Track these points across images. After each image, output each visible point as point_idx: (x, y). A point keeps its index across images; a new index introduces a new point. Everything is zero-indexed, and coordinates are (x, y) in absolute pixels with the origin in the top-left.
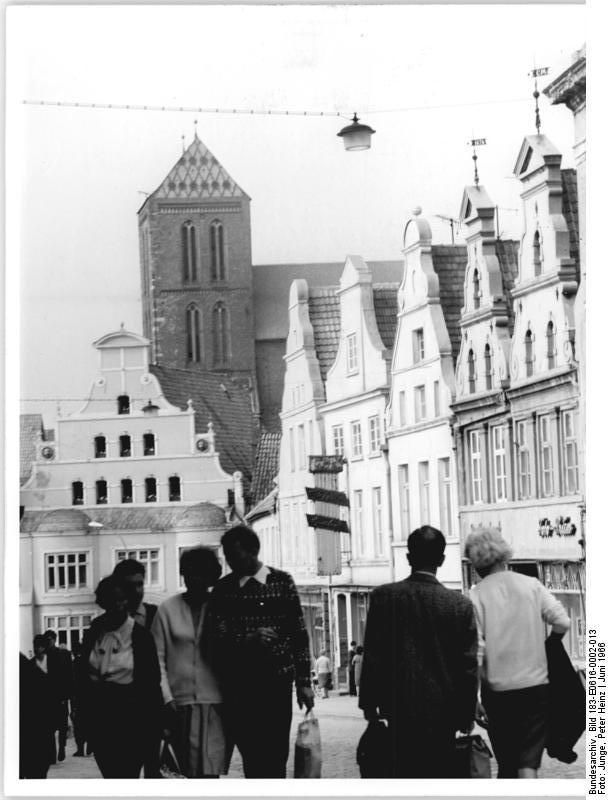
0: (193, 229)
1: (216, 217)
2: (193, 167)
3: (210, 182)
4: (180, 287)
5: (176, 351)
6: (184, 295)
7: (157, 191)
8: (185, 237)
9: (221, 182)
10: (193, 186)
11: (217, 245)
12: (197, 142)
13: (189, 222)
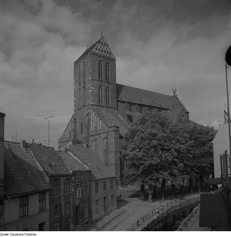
0: (101, 63)
1: (107, 62)
3: (106, 51)
4: (98, 79)
11: (107, 70)
13: (100, 61)
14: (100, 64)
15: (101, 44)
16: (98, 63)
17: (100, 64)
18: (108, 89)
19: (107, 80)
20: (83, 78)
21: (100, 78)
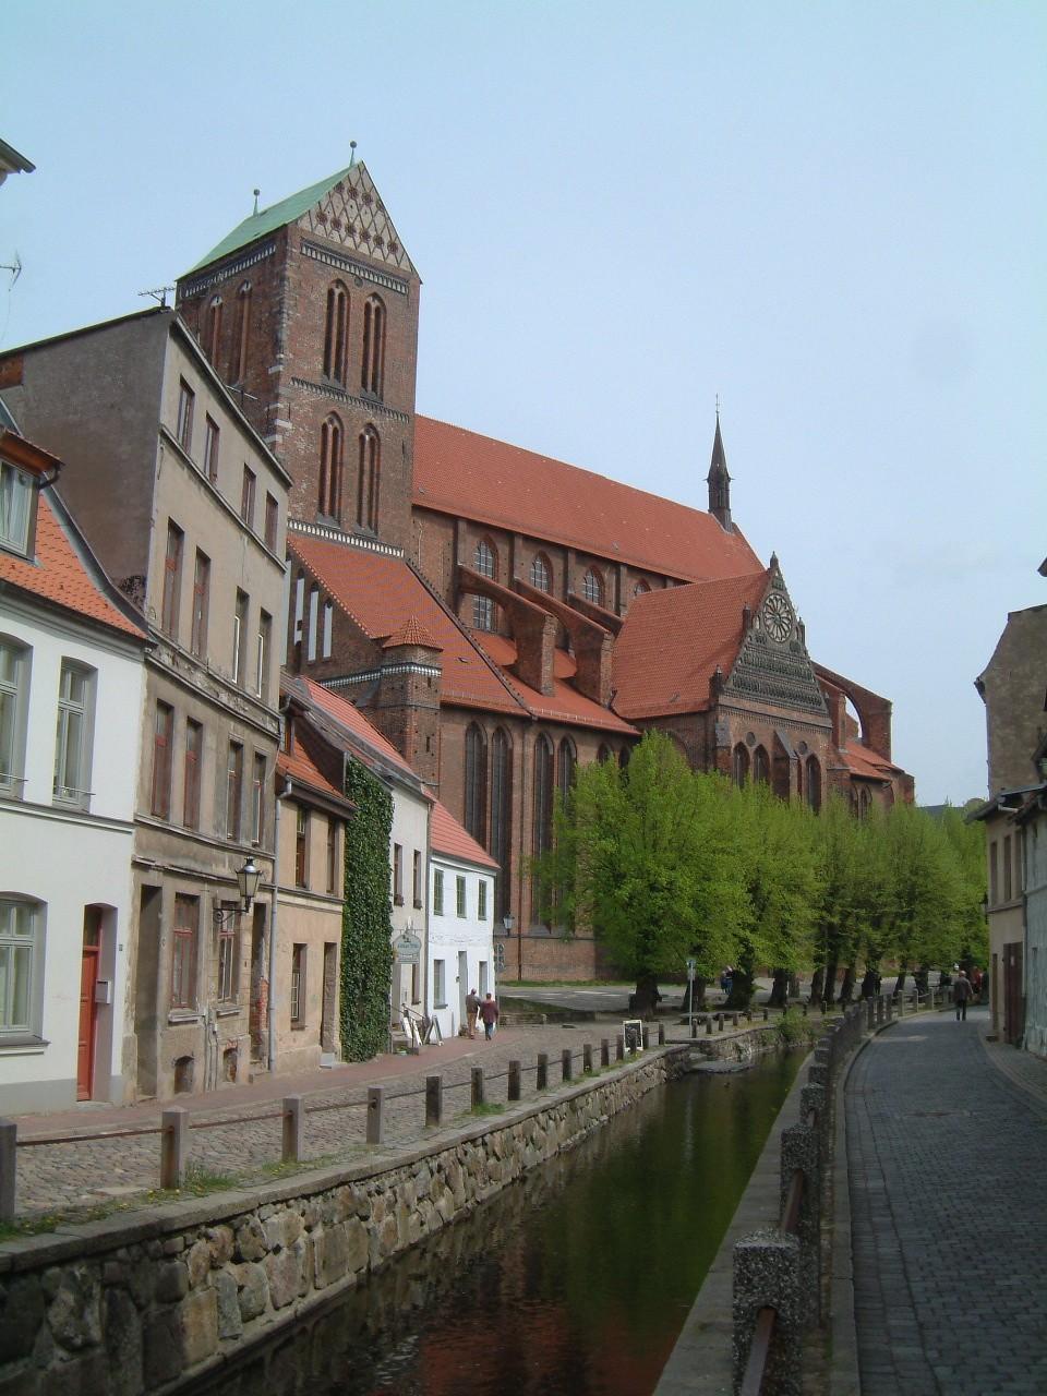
1: (376, 289)
2: (352, 202)
3: (373, 233)
4: (318, 380)
5: (305, 485)
6: (323, 396)
7: (301, 218)
8: (330, 307)
9: (386, 240)
10: (350, 230)
11: (372, 335)
12: (361, 169)
13: (339, 282)
14: (336, 298)
15: (346, 196)
16: (325, 291)
17: (336, 298)
18: (371, 439)
19: (370, 388)
20: (230, 368)
21: (333, 369)
